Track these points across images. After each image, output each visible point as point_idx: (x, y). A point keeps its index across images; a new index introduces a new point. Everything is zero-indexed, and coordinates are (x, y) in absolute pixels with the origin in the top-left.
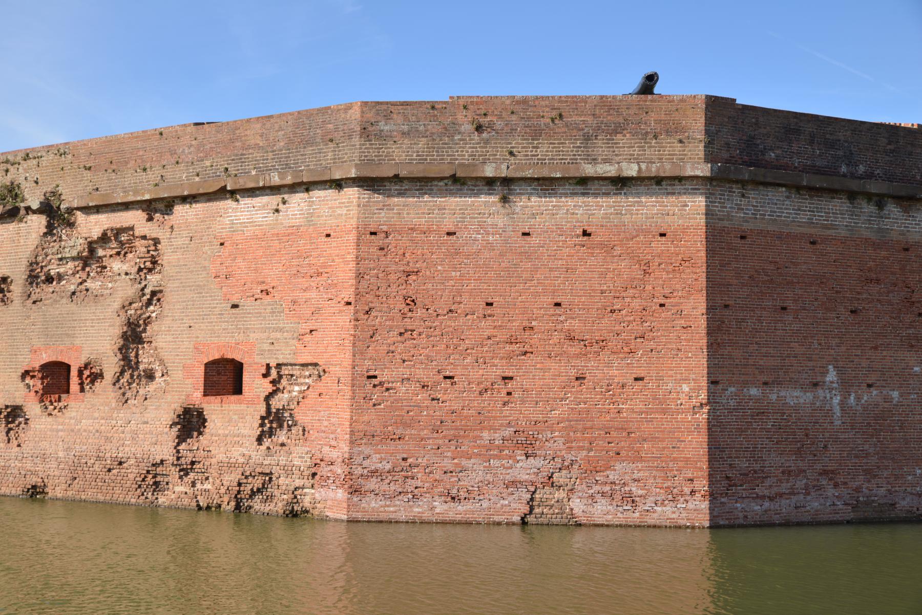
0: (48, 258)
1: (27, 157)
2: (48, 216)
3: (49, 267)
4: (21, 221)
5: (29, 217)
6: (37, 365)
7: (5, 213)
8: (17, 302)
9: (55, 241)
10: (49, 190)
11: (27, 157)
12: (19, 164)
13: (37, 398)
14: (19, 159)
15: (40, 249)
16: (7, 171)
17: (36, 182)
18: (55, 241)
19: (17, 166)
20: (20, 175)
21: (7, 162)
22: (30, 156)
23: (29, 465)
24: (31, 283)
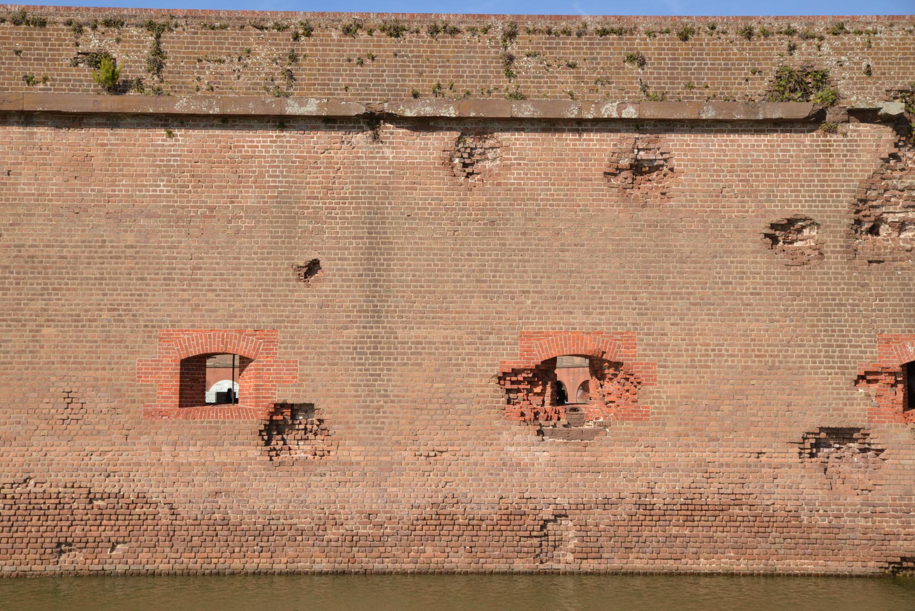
0: (886, 195)
1: (839, 30)
2: (895, 129)
3: (878, 211)
4: (832, 130)
5: (851, 126)
6: (895, 364)
7: (814, 115)
8: (834, 261)
9: (902, 170)
10: (899, 86)
11: (839, 30)
12: (821, 39)
13: (900, 417)
14: (819, 29)
15: (878, 178)
16: (792, 48)
17: (869, 72)
18: (902, 170)
19: (816, 41)
20: (826, 57)
21: (791, 32)
22: (847, 28)
23: (889, 525)
24: (856, 231)
